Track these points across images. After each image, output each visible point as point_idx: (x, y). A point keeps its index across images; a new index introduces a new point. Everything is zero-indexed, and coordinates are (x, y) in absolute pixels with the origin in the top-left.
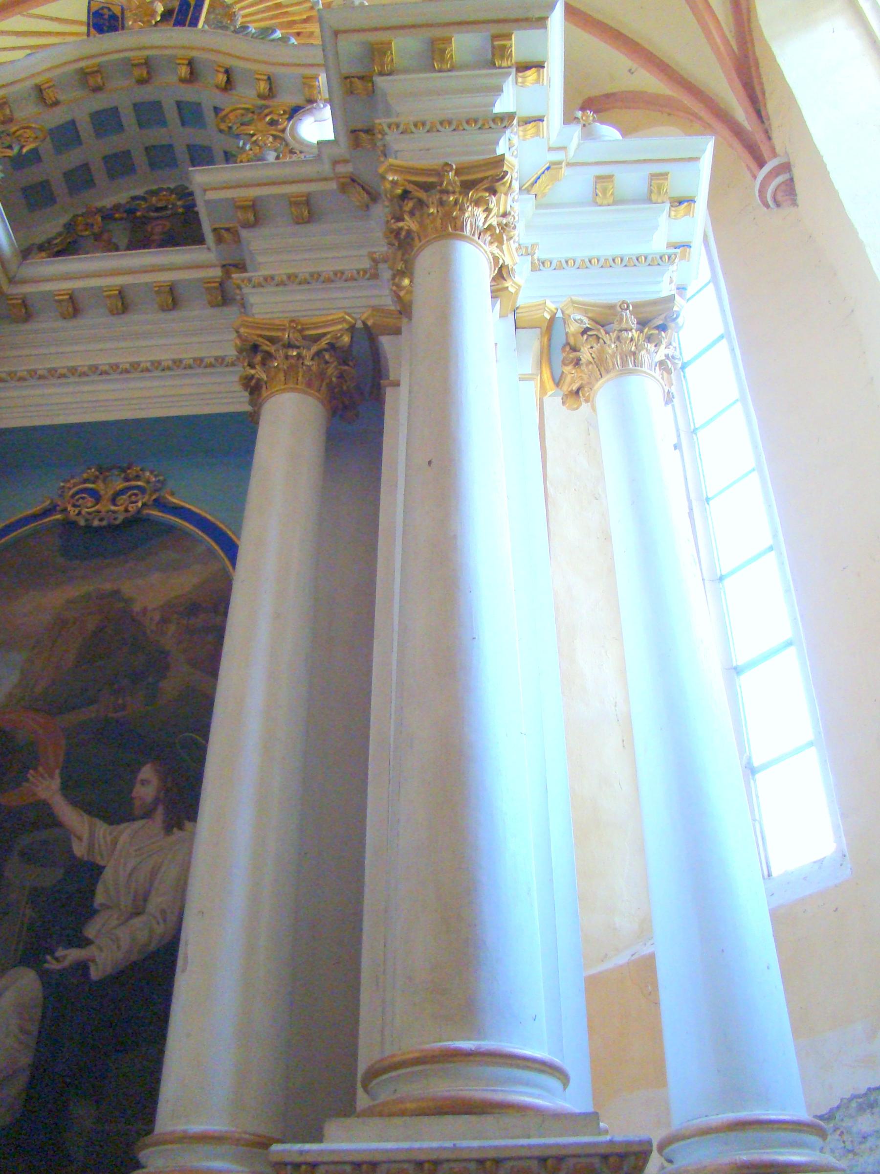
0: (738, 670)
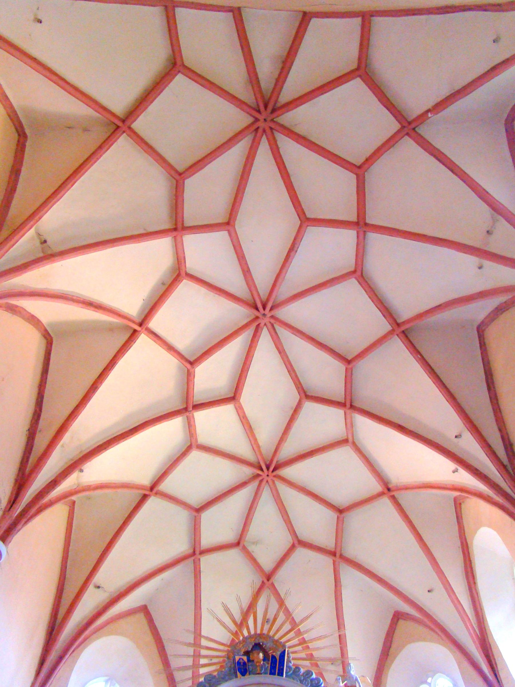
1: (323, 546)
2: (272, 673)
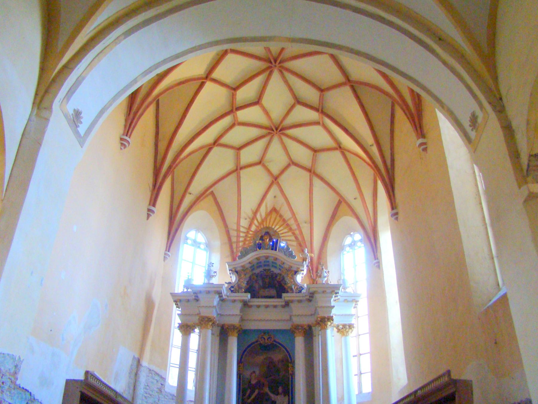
0: (361, 355)
2: (272, 249)
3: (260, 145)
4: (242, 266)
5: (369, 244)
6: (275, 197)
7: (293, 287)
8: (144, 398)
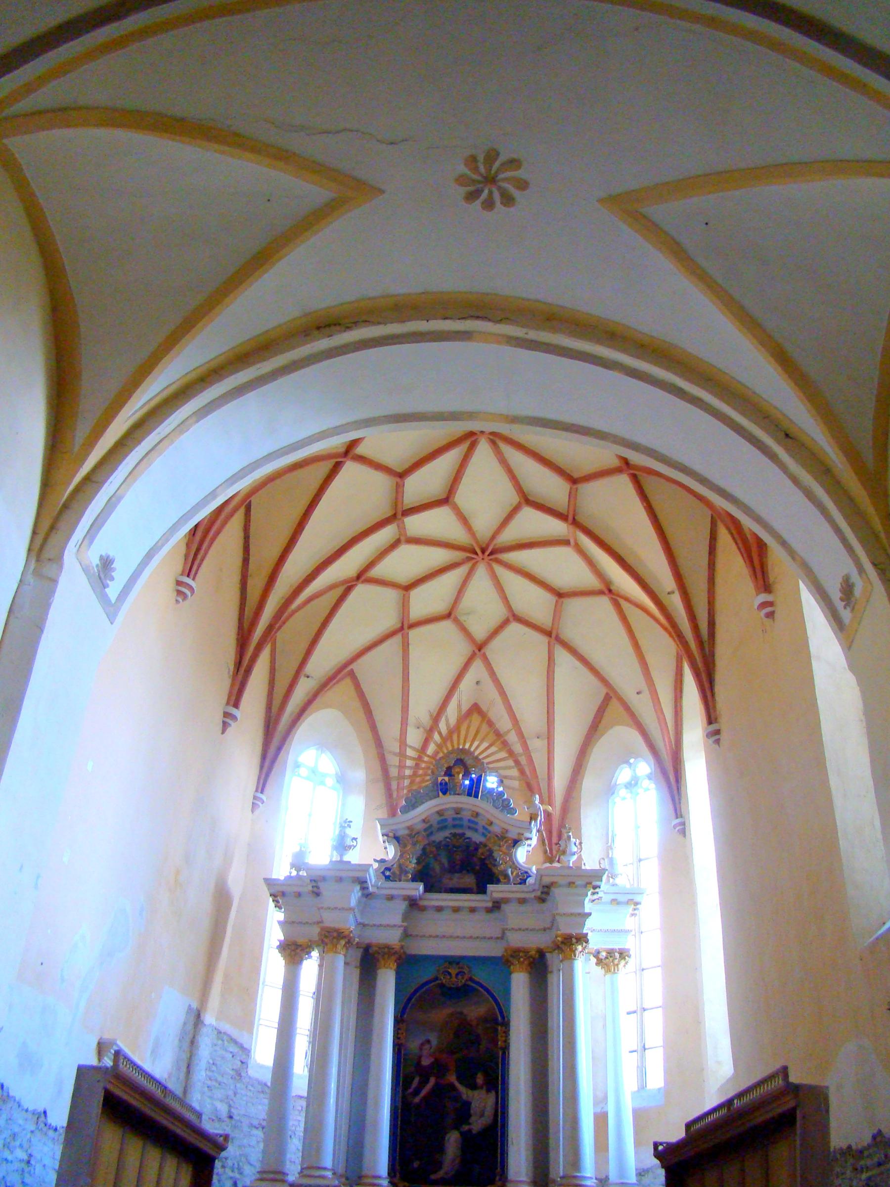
0: (644, 1010)
1: (539, 624)
2: (469, 794)
3: (450, 580)
4: (409, 828)
5: (664, 784)
6: (478, 683)
7: (510, 872)
8: (206, 1089)
